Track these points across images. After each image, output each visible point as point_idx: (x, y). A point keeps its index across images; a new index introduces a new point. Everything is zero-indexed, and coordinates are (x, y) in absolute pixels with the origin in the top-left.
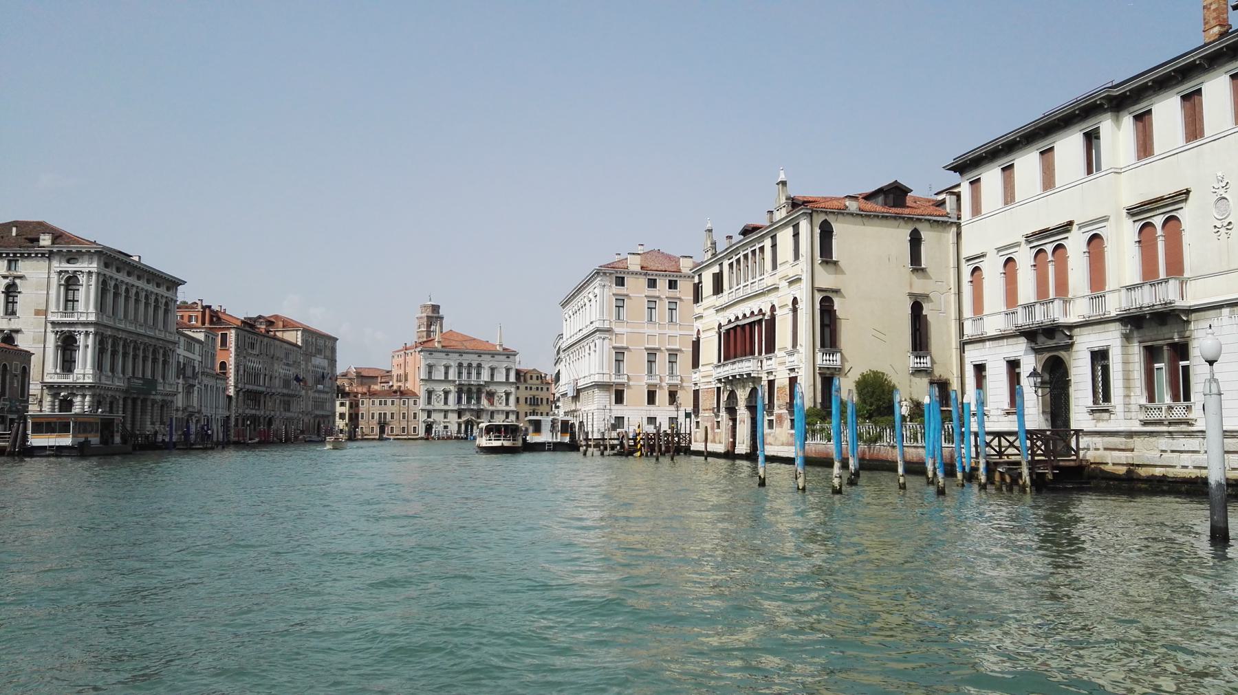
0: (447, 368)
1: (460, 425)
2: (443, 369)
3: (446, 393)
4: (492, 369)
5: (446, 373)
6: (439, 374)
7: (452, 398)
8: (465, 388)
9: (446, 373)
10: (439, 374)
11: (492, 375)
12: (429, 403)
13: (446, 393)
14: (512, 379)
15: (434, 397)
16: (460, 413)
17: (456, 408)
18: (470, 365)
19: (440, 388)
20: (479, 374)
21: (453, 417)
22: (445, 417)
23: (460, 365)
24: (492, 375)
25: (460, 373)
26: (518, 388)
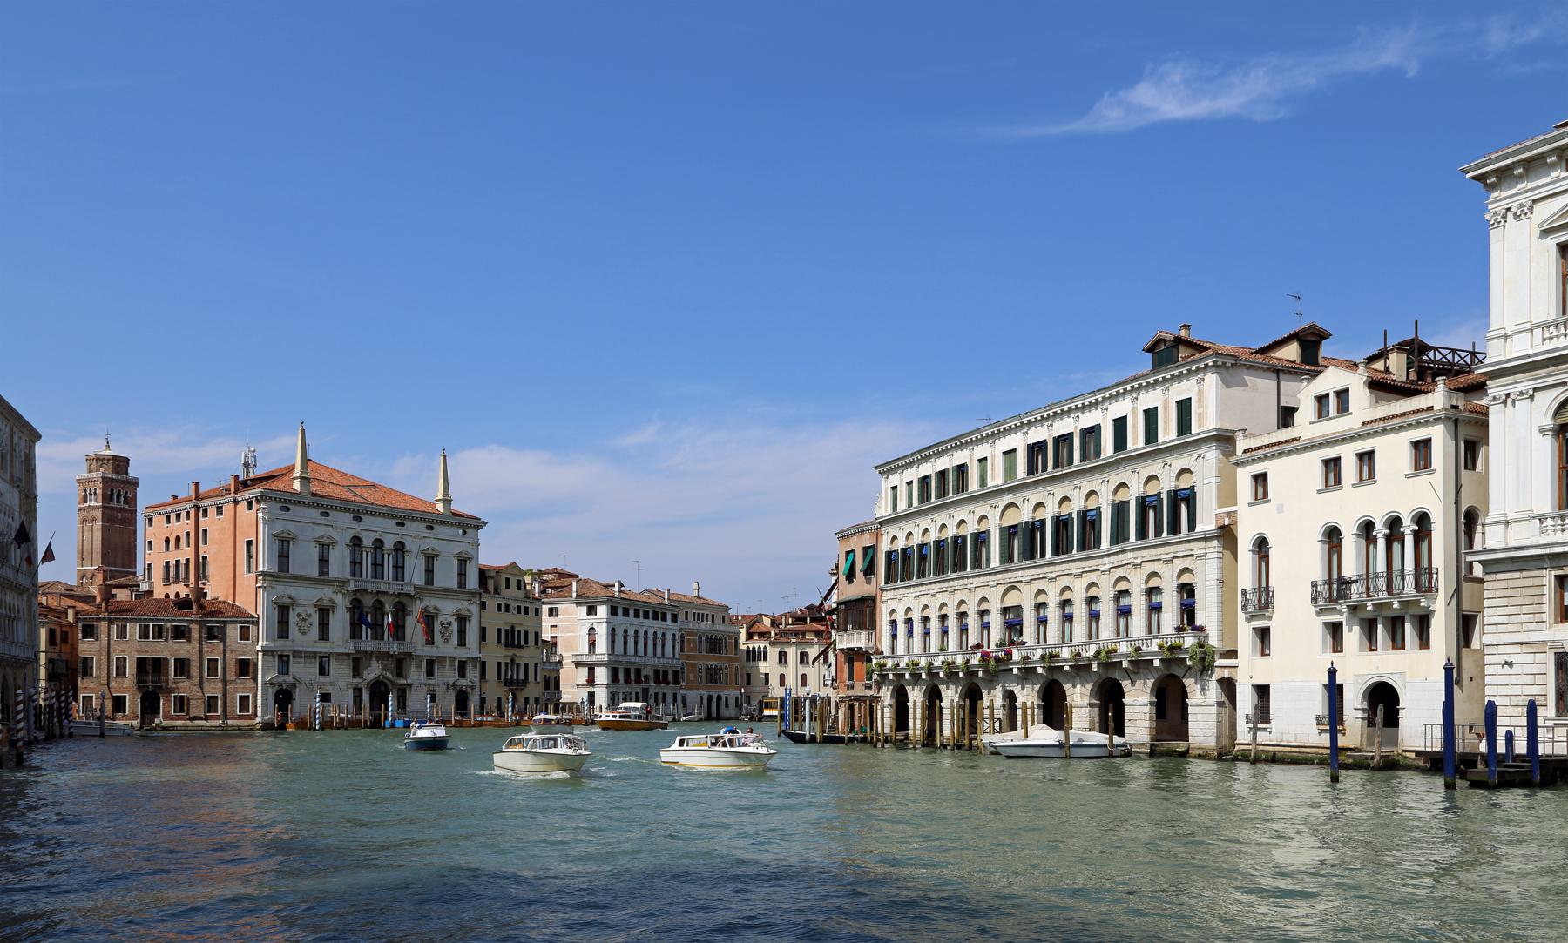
0: (325, 546)
1: (358, 692)
2: (315, 553)
3: (324, 612)
4: (430, 558)
5: (324, 562)
6: (304, 559)
7: (340, 622)
8: (368, 601)
9: (324, 562)
10: (304, 559)
11: (429, 572)
12: (283, 631)
13: (324, 612)
14: (473, 583)
15: (293, 618)
16: (357, 663)
17: (351, 647)
18: (379, 544)
19: (307, 597)
20: (399, 568)
21: (340, 674)
22: (323, 671)
23: (356, 542)
24: (429, 572)
25: (356, 564)
26: (483, 606)
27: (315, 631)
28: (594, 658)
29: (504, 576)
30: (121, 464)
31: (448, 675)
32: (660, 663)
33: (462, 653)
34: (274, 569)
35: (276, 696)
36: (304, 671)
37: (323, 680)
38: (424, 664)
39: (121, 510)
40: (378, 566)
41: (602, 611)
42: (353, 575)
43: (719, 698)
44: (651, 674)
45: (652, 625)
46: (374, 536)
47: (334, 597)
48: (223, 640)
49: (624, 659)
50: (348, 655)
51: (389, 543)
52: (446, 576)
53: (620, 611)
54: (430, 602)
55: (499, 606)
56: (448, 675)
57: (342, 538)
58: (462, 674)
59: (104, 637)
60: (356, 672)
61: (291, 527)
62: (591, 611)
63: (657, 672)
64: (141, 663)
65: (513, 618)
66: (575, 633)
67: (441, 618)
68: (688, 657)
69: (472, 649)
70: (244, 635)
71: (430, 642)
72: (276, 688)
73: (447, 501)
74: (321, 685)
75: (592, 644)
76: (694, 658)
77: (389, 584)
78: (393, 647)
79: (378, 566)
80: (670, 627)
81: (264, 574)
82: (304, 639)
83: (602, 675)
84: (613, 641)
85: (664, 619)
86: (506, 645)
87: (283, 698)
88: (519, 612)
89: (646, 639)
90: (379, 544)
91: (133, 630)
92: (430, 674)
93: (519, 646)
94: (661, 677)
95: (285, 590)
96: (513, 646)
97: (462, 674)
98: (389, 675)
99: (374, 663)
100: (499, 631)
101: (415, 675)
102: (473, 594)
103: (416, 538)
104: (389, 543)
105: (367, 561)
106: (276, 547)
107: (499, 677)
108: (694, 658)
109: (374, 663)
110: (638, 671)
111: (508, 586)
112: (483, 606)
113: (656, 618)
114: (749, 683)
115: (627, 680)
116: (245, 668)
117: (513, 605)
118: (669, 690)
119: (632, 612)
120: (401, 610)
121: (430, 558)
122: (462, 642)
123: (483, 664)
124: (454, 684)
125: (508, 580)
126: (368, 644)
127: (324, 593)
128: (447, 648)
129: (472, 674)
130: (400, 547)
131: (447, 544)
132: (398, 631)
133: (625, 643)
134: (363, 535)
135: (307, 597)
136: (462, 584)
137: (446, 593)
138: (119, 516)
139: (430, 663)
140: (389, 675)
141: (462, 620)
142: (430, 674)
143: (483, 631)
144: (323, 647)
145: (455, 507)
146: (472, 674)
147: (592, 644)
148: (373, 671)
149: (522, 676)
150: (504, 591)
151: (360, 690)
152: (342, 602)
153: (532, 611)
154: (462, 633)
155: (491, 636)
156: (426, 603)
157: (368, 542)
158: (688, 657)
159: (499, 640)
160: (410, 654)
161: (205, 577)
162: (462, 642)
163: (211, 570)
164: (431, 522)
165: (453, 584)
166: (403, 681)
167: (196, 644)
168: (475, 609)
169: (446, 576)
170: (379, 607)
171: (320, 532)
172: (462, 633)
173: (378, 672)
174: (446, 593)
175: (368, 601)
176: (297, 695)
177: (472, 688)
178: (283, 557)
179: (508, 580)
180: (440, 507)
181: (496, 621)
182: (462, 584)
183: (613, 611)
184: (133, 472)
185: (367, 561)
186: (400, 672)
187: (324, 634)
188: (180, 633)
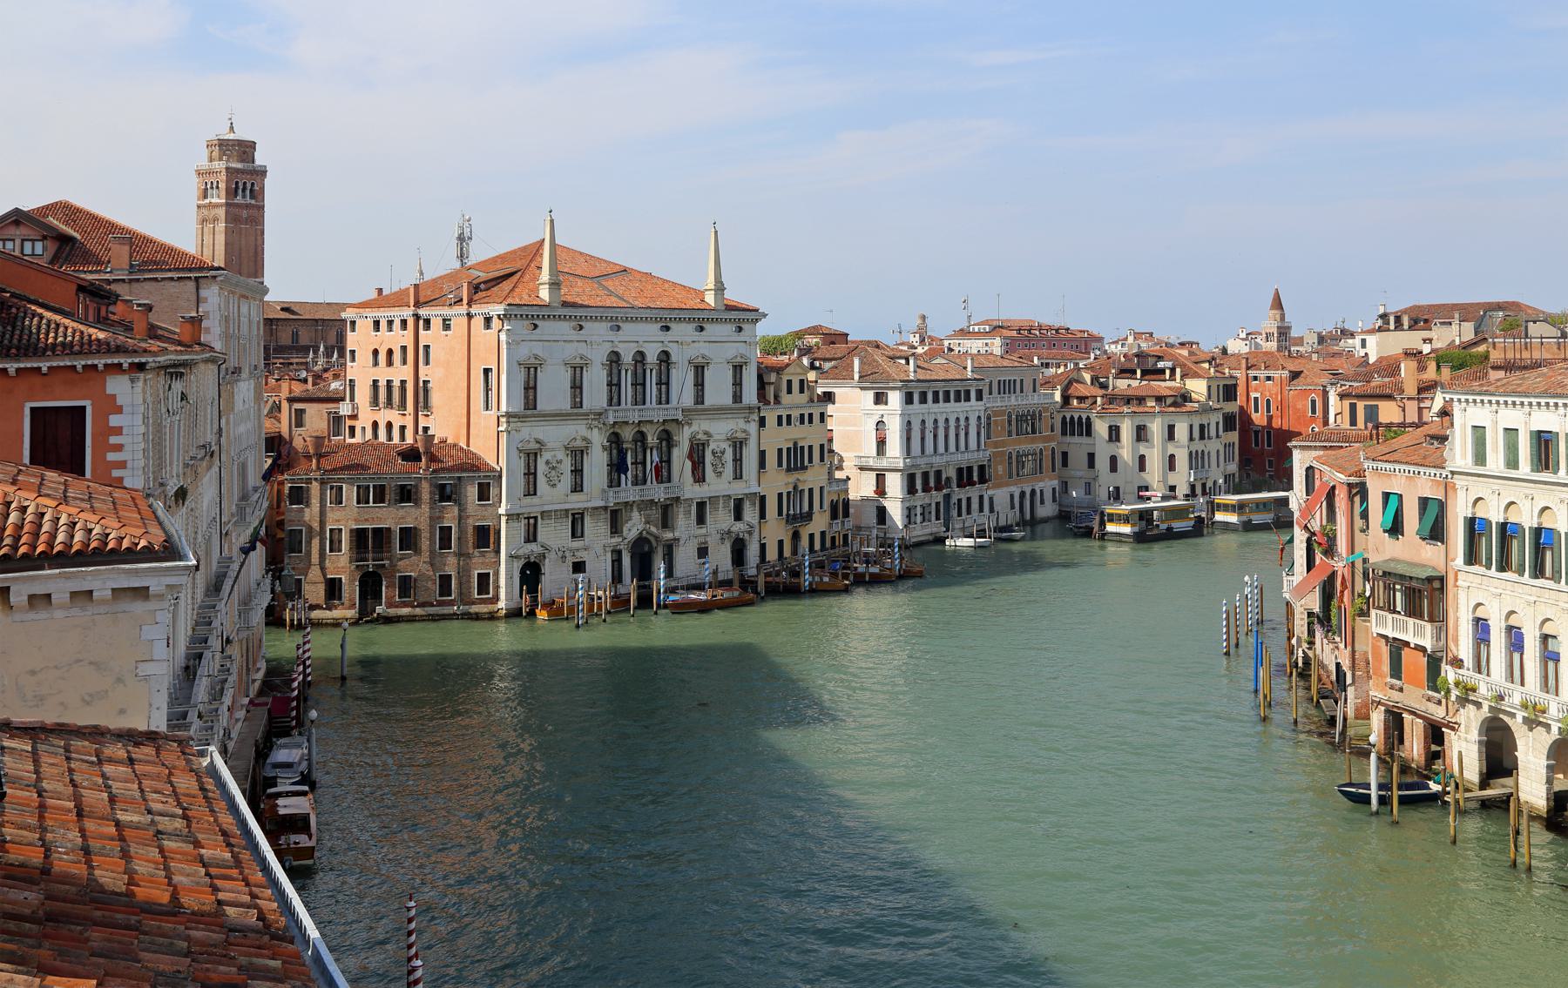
3: (578, 455)
4: (699, 370)
5: (577, 387)
6: (553, 391)
7: (597, 464)
8: (628, 434)
9: (577, 387)
10: (553, 391)
11: (699, 384)
13: (578, 455)
18: (640, 357)
19: (556, 436)
20: (664, 383)
21: (597, 531)
22: (577, 532)
23: (614, 359)
24: (699, 384)
25: (614, 385)
26: (762, 422)
27: (567, 480)
28: (884, 463)
29: (785, 378)
30: (245, 149)
31: (721, 519)
32: (964, 459)
33: (738, 489)
34: (519, 407)
35: (522, 572)
36: (554, 535)
37: (577, 544)
38: (694, 508)
39: (247, 206)
40: (639, 384)
41: (895, 398)
42: (610, 404)
43: (1033, 492)
44: (952, 473)
45: (954, 409)
46: (634, 348)
47: (587, 434)
48: (459, 502)
49: (922, 461)
50: (606, 508)
51: (652, 357)
52: (718, 390)
53: (916, 398)
54: (700, 426)
55: (780, 418)
56: (721, 519)
57: (599, 356)
58: (738, 517)
59: (315, 502)
60: (615, 529)
61: (538, 349)
62: (880, 399)
63: (960, 471)
64: (359, 536)
65: (796, 432)
66: (864, 435)
67: (712, 446)
68: (996, 445)
69: (750, 484)
70: (483, 494)
71: (699, 477)
72: (522, 562)
73: (720, 288)
74: (574, 551)
75: (881, 443)
76: (1003, 444)
77: (654, 411)
78: (658, 492)
79: (639, 384)
80: (974, 408)
81: (508, 415)
82: (554, 494)
83: (895, 484)
84: (908, 439)
85: (968, 399)
86: (789, 470)
87: (531, 574)
88: (802, 422)
89: (947, 429)
90: (640, 357)
91: (350, 493)
92: (701, 520)
93: (804, 468)
94: (965, 477)
95: (532, 432)
96: (796, 469)
97: (738, 517)
98: (653, 529)
99: (635, 514)
100: (780, 451)
101: (684, 524)
102: (750, 409)
103: (685, 344)
104: (652, 357)
105: (627, 381)
106: (521, 377)
107: (780, 514)
108: (1003, 444)
109: (635, 514)
110: (938, 473)
111: (789, 391)
112: (762, 422)
113: (958, 400)
114: (1065, 463)
115: (926, 489)
116: (485, 537)
117: (795, 414)
118: (973, 493)
119: (930, 397)
120: (667, 439)
121: (699, 370)
122: (738, 475)
123: (763, 499)
124: (729, 532)
125: (789, 382)
126: (628, 492)
127: (575, 430)
128: (719, 484)
129: (751, 514)
130: (665, 357)
131: (719, 347)
132: (663, 473)
133: (923, 439)
134: (621, 349)
135: (556, 436)
136: (737, 397)
137: (719, 411)
138: (245, 213)
139: (701, 506)
140: (653, 529)
141: (738, 445)
142: (701, 520)
143: (762, 454)
144: (577, 502)
145: (732, 295)
146: (751, 514)
147: (881, 443)
148: (634, 526)
149: (806, 508)
150: (786, 399)
151: (620, 552)
152: (598, 439)
153: (816, 418)
154: (738, 460)
155: (772, 459)
156: (695, 428)
157: (627, 358)
158: (996, 445)
159: (780, 464)
160: (678, 498)
161: (427, 406)
162: (738, 475)
163: (435, 398)
164: (700, 320)
165: (727, 399)
166: (669, 535)
167: (425, 508)
168: (753, 427)
169: (718, 390)
170: (641, 437)
171: (571, 351)
172: (738, 460)
173: (641, 527)
174: (719, 411)
175: (628, 434)
176: (547, 568)
177: (750, 533)
178: (530, 389)
179: (789, 382)
180: (710, 299)
181: (776, 438)
182: (737, 397)
183: (909, 399)
184: (260, 159)
185: (627, 381)
186: (666, 523)
187: (577, 488)
188: (406, 494)
